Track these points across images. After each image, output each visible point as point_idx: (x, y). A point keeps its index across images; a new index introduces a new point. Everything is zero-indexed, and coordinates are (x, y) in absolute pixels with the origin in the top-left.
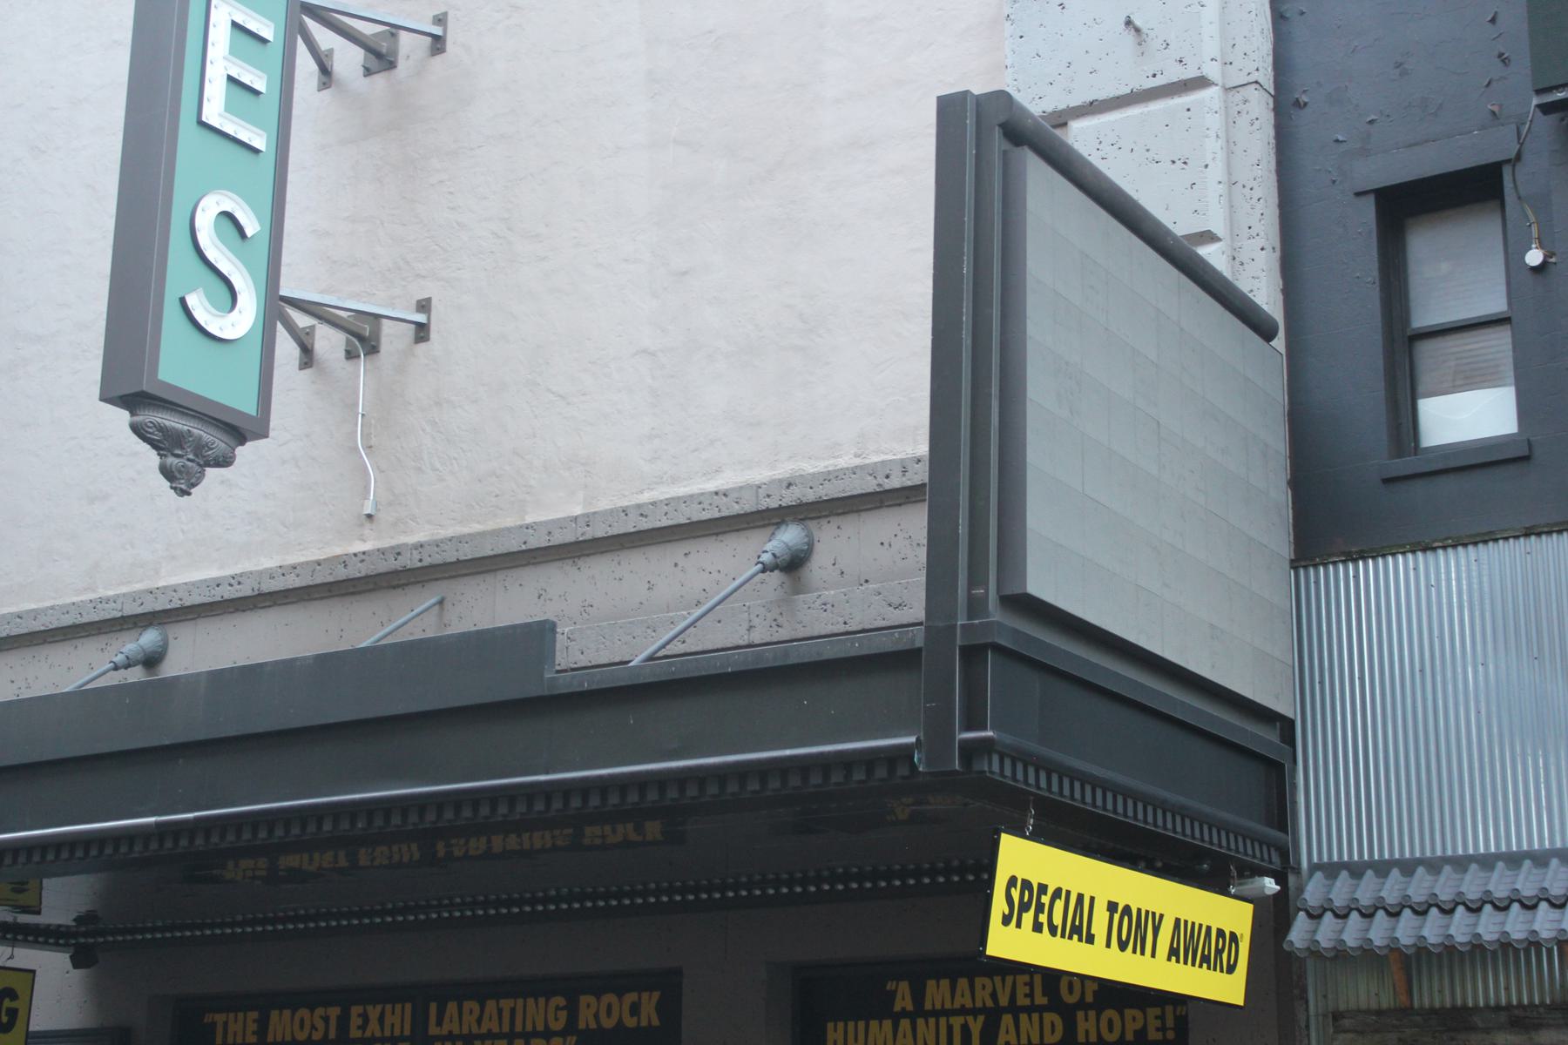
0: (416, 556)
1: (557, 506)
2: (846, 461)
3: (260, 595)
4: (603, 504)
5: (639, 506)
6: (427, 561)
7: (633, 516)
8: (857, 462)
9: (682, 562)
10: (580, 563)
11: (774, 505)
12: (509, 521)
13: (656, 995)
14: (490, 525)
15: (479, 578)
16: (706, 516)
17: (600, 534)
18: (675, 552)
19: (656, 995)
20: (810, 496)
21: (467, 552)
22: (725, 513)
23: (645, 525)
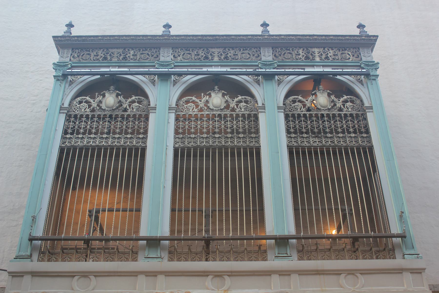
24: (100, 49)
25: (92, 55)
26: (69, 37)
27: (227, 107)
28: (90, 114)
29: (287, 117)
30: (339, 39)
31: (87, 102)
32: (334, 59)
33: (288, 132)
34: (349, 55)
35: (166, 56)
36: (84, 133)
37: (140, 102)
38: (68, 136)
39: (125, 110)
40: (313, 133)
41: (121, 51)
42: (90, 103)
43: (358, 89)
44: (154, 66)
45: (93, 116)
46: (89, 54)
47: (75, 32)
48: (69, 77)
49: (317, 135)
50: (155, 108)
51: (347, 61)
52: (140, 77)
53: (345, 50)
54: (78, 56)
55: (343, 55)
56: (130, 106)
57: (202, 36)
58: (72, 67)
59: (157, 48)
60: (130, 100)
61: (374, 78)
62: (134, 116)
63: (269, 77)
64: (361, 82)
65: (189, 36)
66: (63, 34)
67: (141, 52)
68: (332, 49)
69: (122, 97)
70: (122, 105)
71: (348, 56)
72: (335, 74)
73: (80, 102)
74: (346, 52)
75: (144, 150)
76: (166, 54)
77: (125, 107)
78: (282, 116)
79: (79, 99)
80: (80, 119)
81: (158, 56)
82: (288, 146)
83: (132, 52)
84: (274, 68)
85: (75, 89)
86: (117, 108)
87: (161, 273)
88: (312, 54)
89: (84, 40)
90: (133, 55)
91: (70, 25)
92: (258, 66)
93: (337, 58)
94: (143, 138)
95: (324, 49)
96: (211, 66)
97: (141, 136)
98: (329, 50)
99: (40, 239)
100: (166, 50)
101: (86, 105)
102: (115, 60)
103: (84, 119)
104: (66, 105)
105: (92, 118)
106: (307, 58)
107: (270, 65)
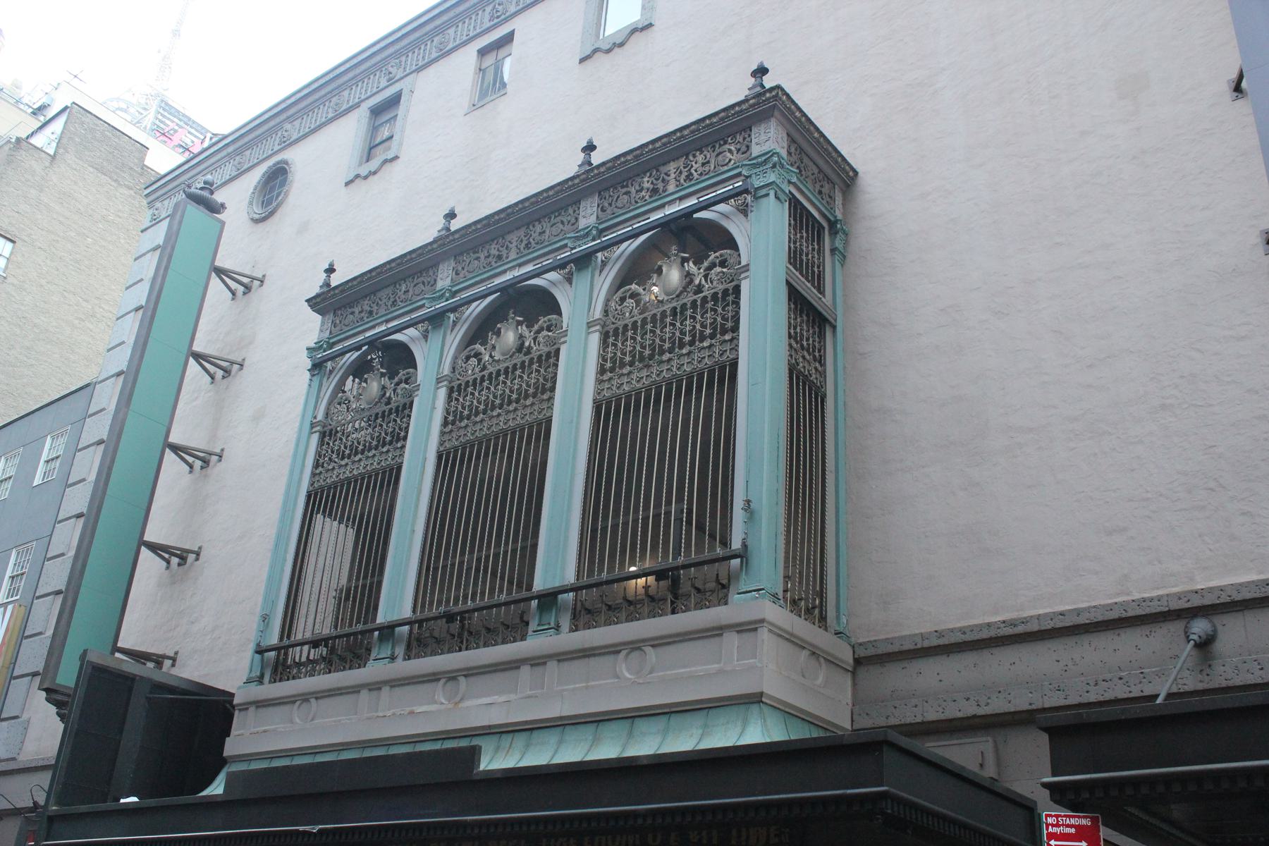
24: (645, 173)
25: (482, 256)
26: (592, 170)
27: (520, 348)
28: (639, 318)
29: (605, 336)
30: (707, 125)
31: (634, 295)
32: (701, 174)
33: (602, 370)
34: (730, 151)
35: (588, 216)
36: (692, 343)
37: (723, 264)
38: (605, 377)
39: (699, 289)
40: (642, 359)
41: (521, 232)
42: (638, 294)
43: (737, 228)
44: (423, 306)
45: (644, 321)
46: (628, 193)
47: (597, 158)
48: (599, 255)
49: (645, 361)
50: (746, 268)
51: (726, 168)
52: (722, 207)
53: (725, 143)
54: (610, 205)
55: (720, 158)
56: (706, 277)
57: (486, 217)
58: (601, 232)
59: (744, 130)
60: (706, 264)
61: (763, 192)
62: (715, 296)
63: (583, 261)
64: (744, 211)
65: (516, 204)
66: (747, 92)
67: (717, 151)
68: (702, 152)
69: (691, 264)
70: (691, 281)
71: (728, 155)
72: (688, 214)
73: (623, 299)
74: (727, 146)
75: (734, 365)
76: (763, 137)
77: (697, 282)
78: (595, 339)
79: (620, 293)
80: (724, 298)
81: (748, 147)
82: (595, 401)
83: (700, 158)
84: (594, 240)
85: (461, 331)
86: (685, 289)
87: (385, 683)
88: (663, 180)
89: (636, 157)
90: (703, 164)
91: (590, 148)
92: (566, 246)
93: (707, 169)
94: (731, 340)
95: (687, 156)
96: (504, 272)
97: (727, 337)
98: (694, 156)
99: (571, 590)
100: (763, 126)
101: (630, 302)
102: (671, 188)
103: (710, 305)
104: (598, 313)
105: (547, 360)
106: (655, 191)
107: (587, 234)
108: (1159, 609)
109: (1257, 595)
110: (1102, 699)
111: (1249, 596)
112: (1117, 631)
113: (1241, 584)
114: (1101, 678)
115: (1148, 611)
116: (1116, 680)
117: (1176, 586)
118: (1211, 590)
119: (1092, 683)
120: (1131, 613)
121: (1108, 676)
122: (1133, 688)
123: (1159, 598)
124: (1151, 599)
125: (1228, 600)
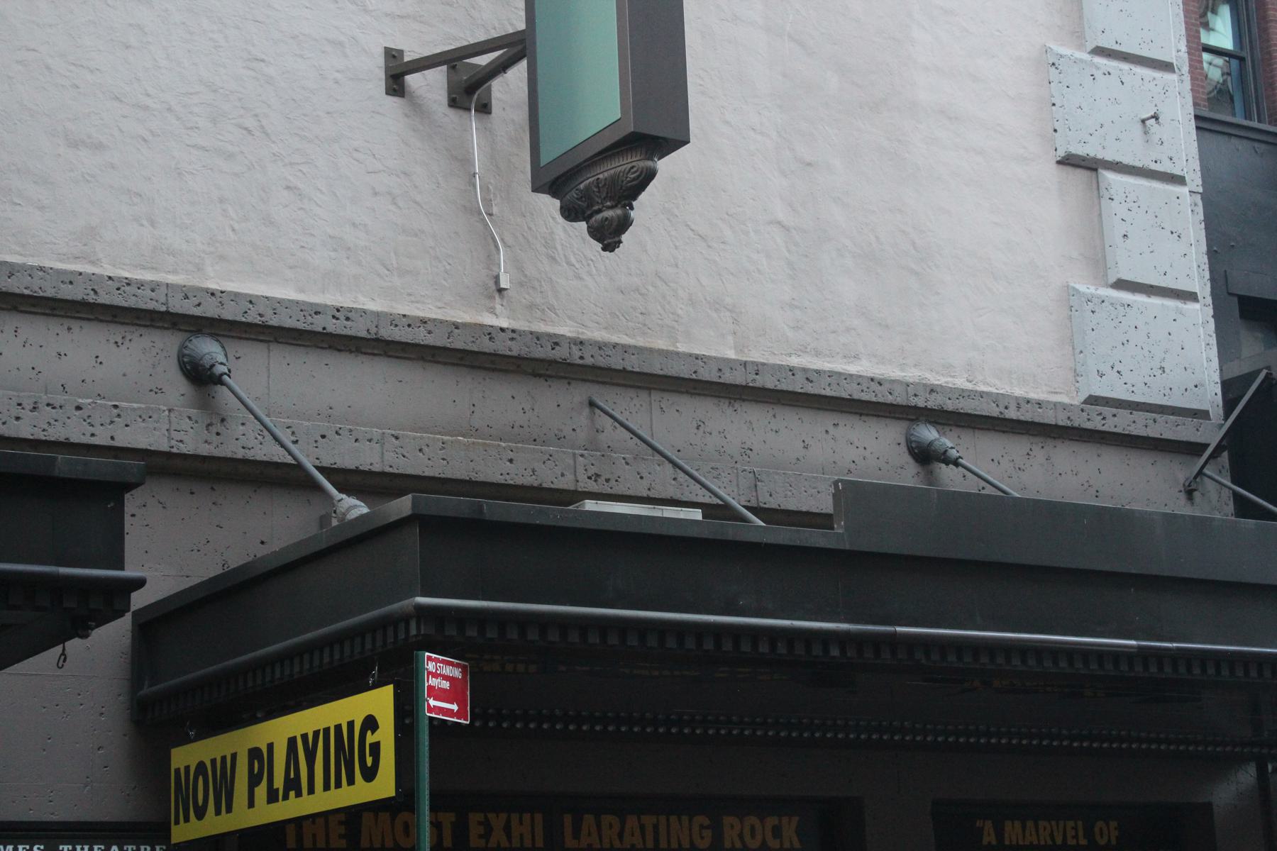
0: (576, 353)
1: (711, 343)
2: (961, 383)
3: (377, 340)
4: (755, 356)
5: (805, 370)
6: (589, 361)
7: (799, 376)
8: (969, 386)
9: (832, 430)
10: (737, 405)
11: (921, 404)
12: (661, 344)
13: (796, 819)
14: (640, 342)
15: (632, 393)
16: (865, 397)
17: (770, 385)
18: (826, 420)
19: (796, 819)
20: (950, 406)
21: (633, 364)
22: (881, 400)
23: (810, 389)
108: (151, 306)
109: (300, 326)
110: (41, 436)
111: (289, 323)
112: (67, 322)
113: (280, 301)
114: (45, 398)
115: (131, 302)
116: (70, 409)
117: (175, 272)
118: (236, 297)
119: (28, 404)
120: (103, 299)
121: (59, 399)
122: (98, 430)
123: (154, 287)
124: (141, 285)
125: (258, 320)
